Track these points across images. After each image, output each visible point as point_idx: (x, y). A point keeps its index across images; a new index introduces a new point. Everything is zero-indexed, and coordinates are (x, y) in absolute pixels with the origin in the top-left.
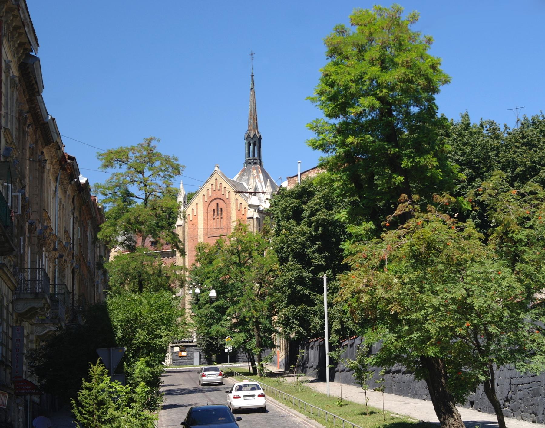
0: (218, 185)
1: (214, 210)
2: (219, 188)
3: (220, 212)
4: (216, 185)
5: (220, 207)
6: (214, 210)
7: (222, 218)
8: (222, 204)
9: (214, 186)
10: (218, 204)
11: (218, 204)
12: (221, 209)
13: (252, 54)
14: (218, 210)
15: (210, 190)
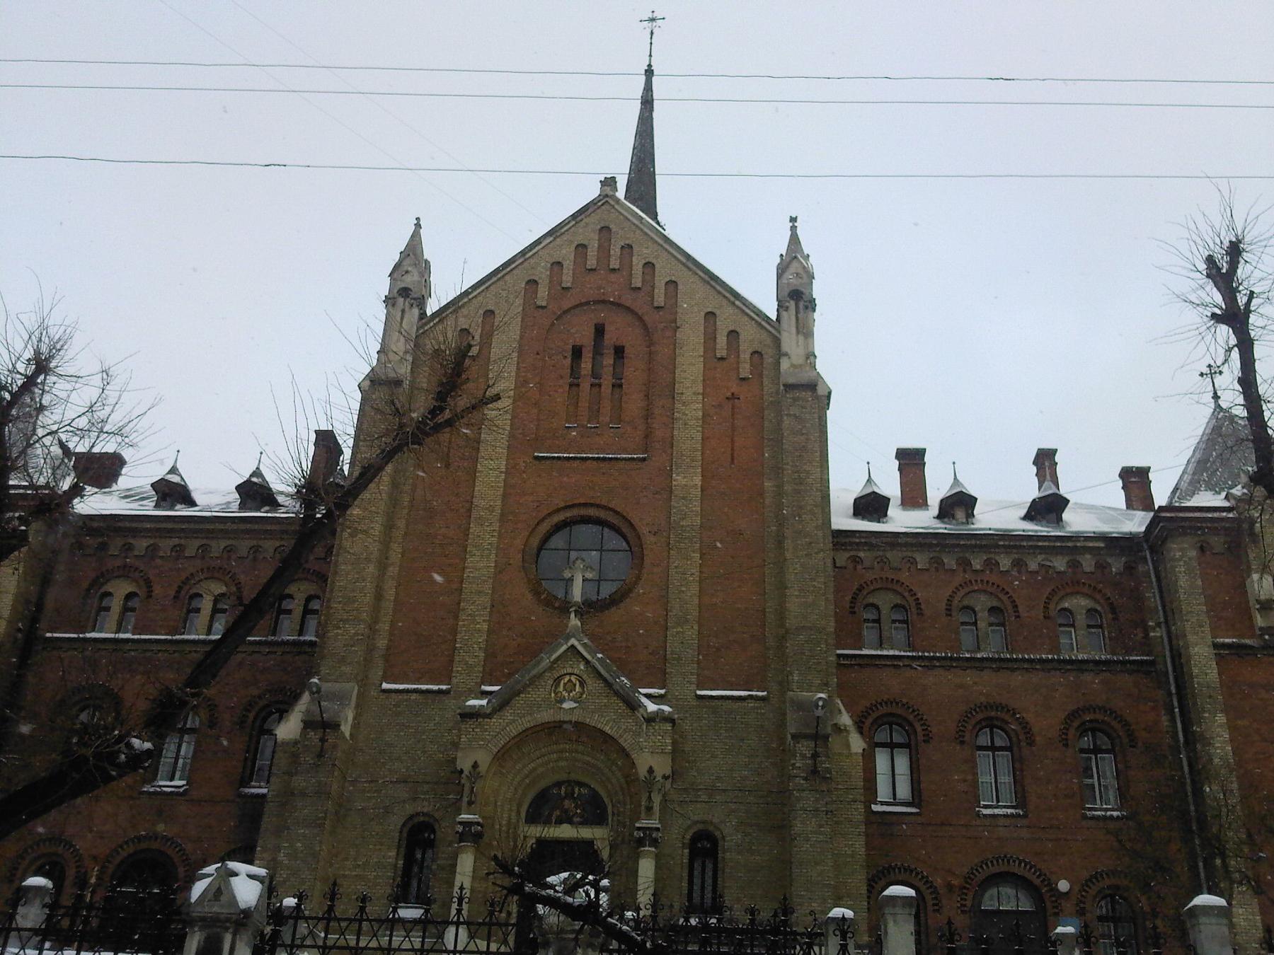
0: (615, 251)
1: (577, 352)
2: (614, 264)
3: (608, 360)
4: (604, 250)
5: (610, 338)
6: (577, 352)
7: (618, 386)
8: (619, 330)
9: (592, 254)
10: (600, 330)
11: (600, 330)
12: (619, 352)
13: (653, 20)
14: (598, 351)
15: (568, 264)
